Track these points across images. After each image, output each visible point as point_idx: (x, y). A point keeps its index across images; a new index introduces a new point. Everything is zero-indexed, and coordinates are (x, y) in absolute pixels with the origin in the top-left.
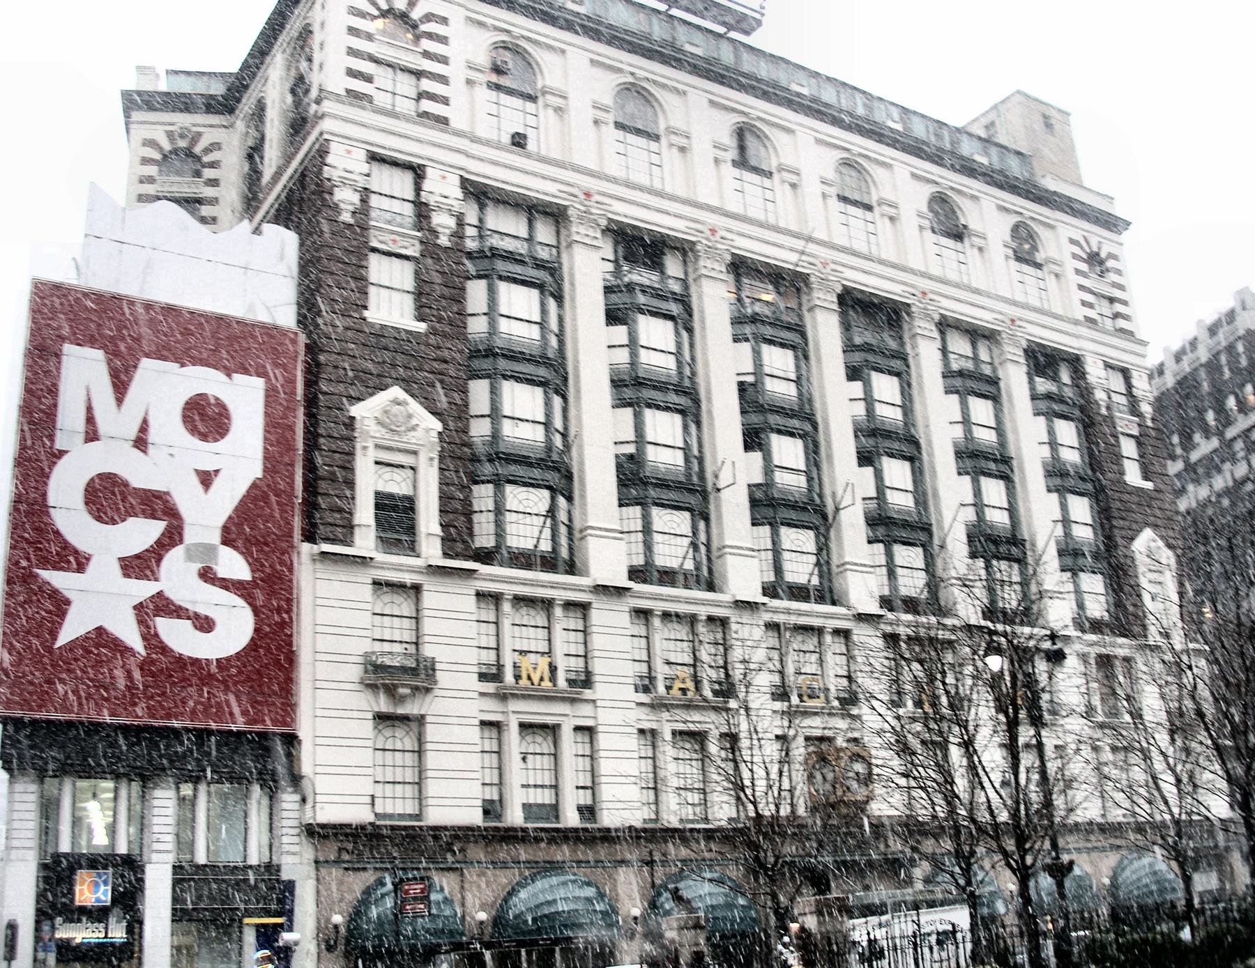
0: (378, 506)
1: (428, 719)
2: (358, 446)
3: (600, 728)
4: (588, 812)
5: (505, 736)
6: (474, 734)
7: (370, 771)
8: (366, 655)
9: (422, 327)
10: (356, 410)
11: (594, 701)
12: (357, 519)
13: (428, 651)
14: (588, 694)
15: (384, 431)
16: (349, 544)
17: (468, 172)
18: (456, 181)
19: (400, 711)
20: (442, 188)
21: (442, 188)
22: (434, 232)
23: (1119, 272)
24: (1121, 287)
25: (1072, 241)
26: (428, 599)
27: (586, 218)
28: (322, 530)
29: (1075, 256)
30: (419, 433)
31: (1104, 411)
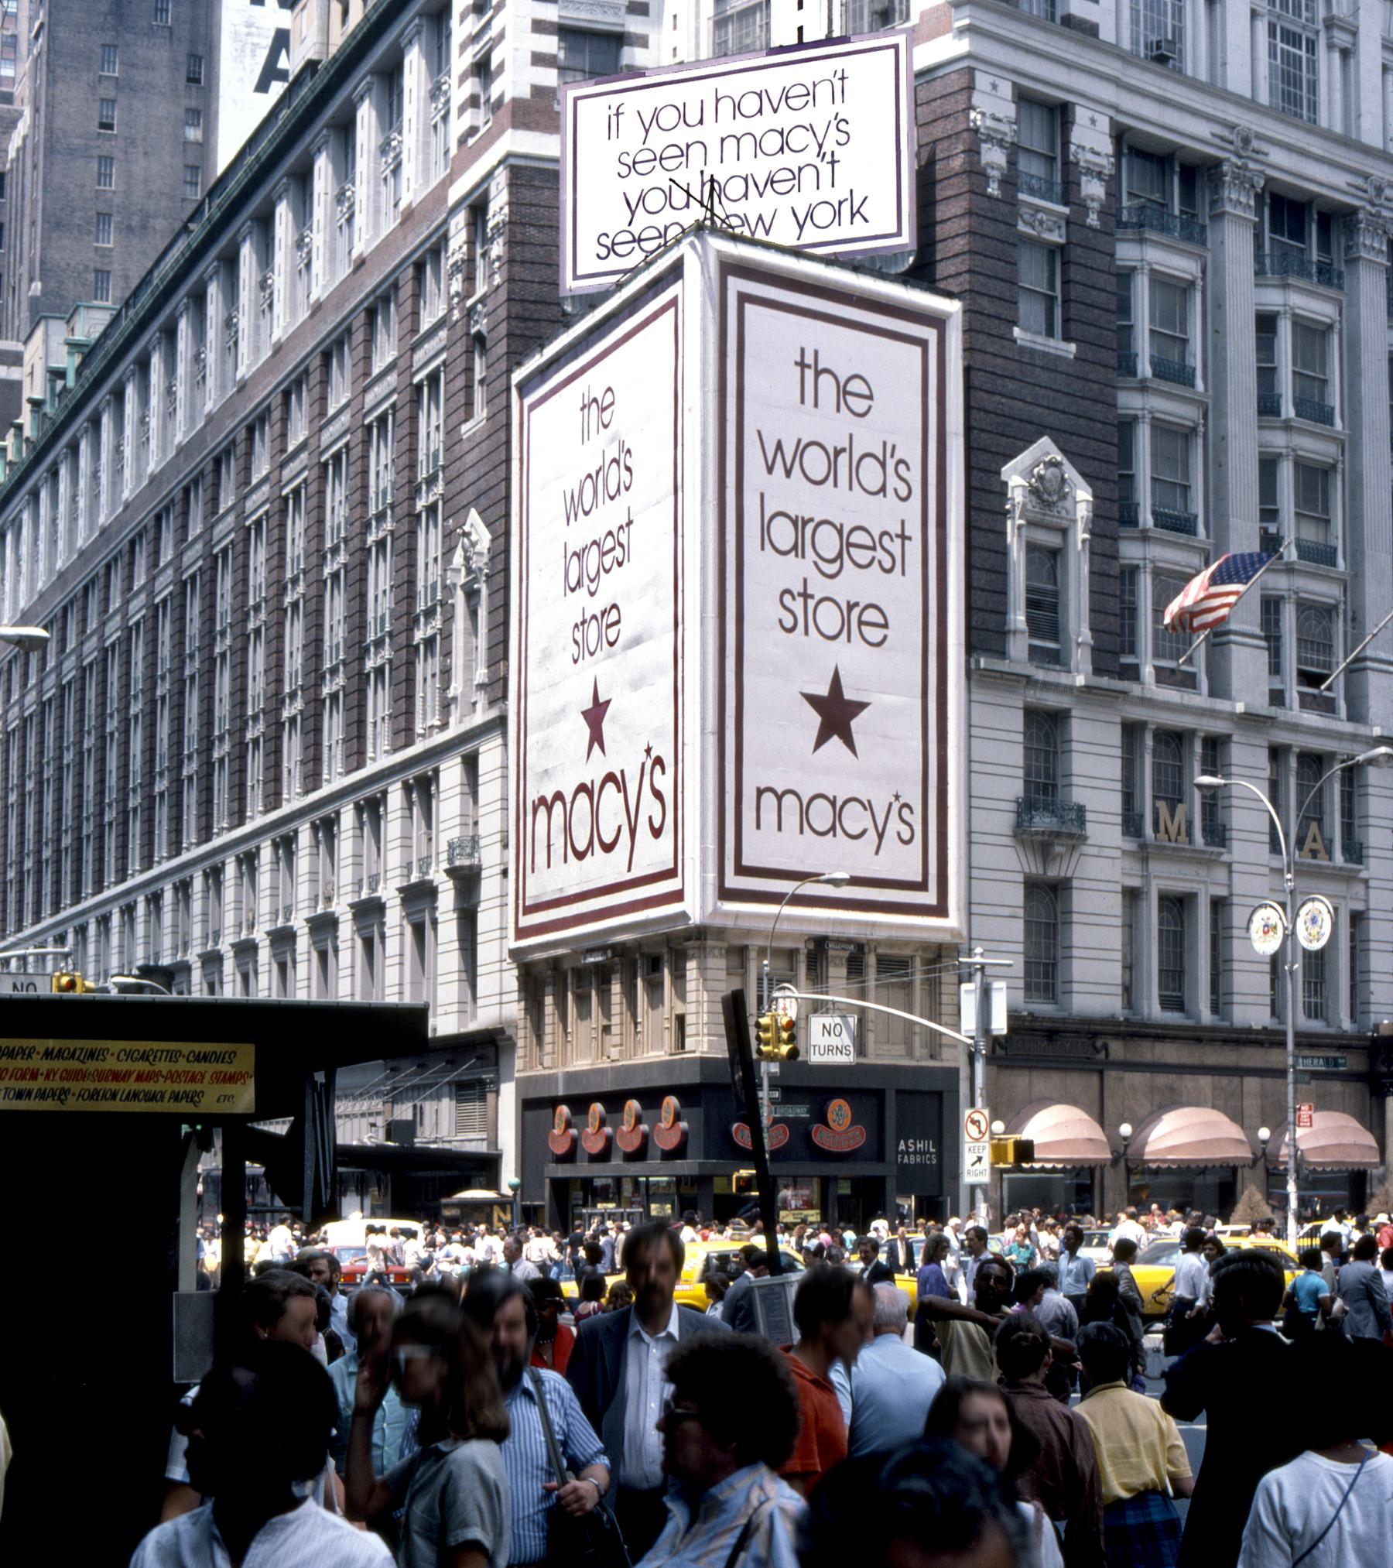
0: (1031, 604)
1: (1075, 883)
6: (1115, 904)
13: (1078, 796)
16: (1002, 654)
18: (1104, 124)
19: (1053, 872)
20: (1091, 138)
21: (1091, 138)
22: (1081, 206)
26: (1079, 729)
27: (1242, 179)
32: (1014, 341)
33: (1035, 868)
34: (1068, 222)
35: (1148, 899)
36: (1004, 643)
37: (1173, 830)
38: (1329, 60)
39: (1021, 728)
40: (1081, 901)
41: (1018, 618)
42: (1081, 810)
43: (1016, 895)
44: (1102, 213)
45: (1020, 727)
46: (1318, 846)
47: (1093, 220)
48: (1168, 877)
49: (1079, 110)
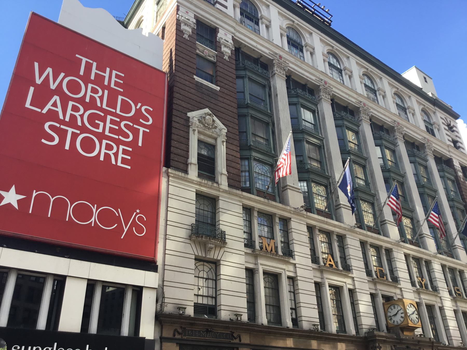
1: (222, 262)
2: (191, 130)
3: (299, 278)
4: (295, 321)
5: (256, 276)
7: (192, 287)
8: (192, 225)
9: (218, 88)
10: (189, 114)
11: (295, 265)
12: (189, 161)
13: (222, 228)
14: (292, 261)
15: (202, 126)
16: (186, 172)
17: (235, 36)
23: (458, 132)
24: (460, 138)
25: (441, 118)
28: (172, 163)
29: (443, 123)
30: (217, 130)
31: (462, 180)
32: (194, 79)
33: (201, 254)
34: (217, 56)
35: (258, 273)
36: (187, 167)
37: (269, 249)
38: (307, 54)
39: (195, 199)
40: (225, 270)
41: (193, 159)
42: (223, 234)
43: (191, 264)
44: (229, 57)
45: (194, 198)
46: (332, 263)
47: (226, 57)
48: (265, 265)
49: (220, 30)
